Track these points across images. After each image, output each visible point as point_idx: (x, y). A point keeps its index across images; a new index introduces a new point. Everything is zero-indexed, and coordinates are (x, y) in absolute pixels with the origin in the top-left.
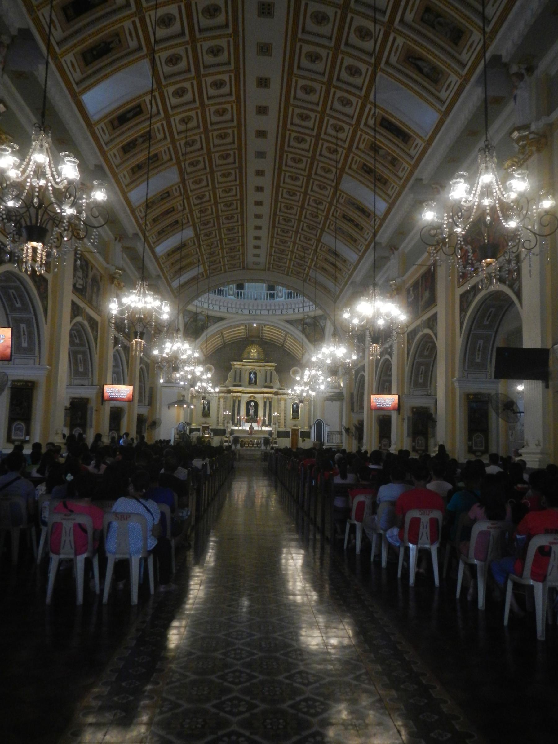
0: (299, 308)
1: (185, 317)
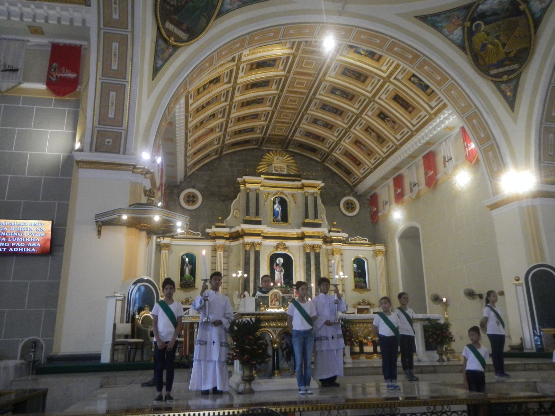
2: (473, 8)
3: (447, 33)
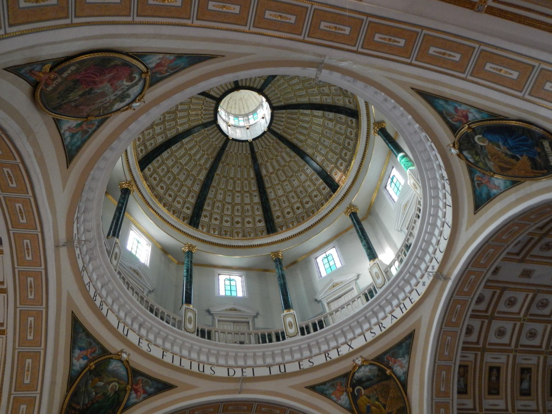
0: (337, 348)
1: (77, 352)
2: (351, 375)
3: (335, 399)
